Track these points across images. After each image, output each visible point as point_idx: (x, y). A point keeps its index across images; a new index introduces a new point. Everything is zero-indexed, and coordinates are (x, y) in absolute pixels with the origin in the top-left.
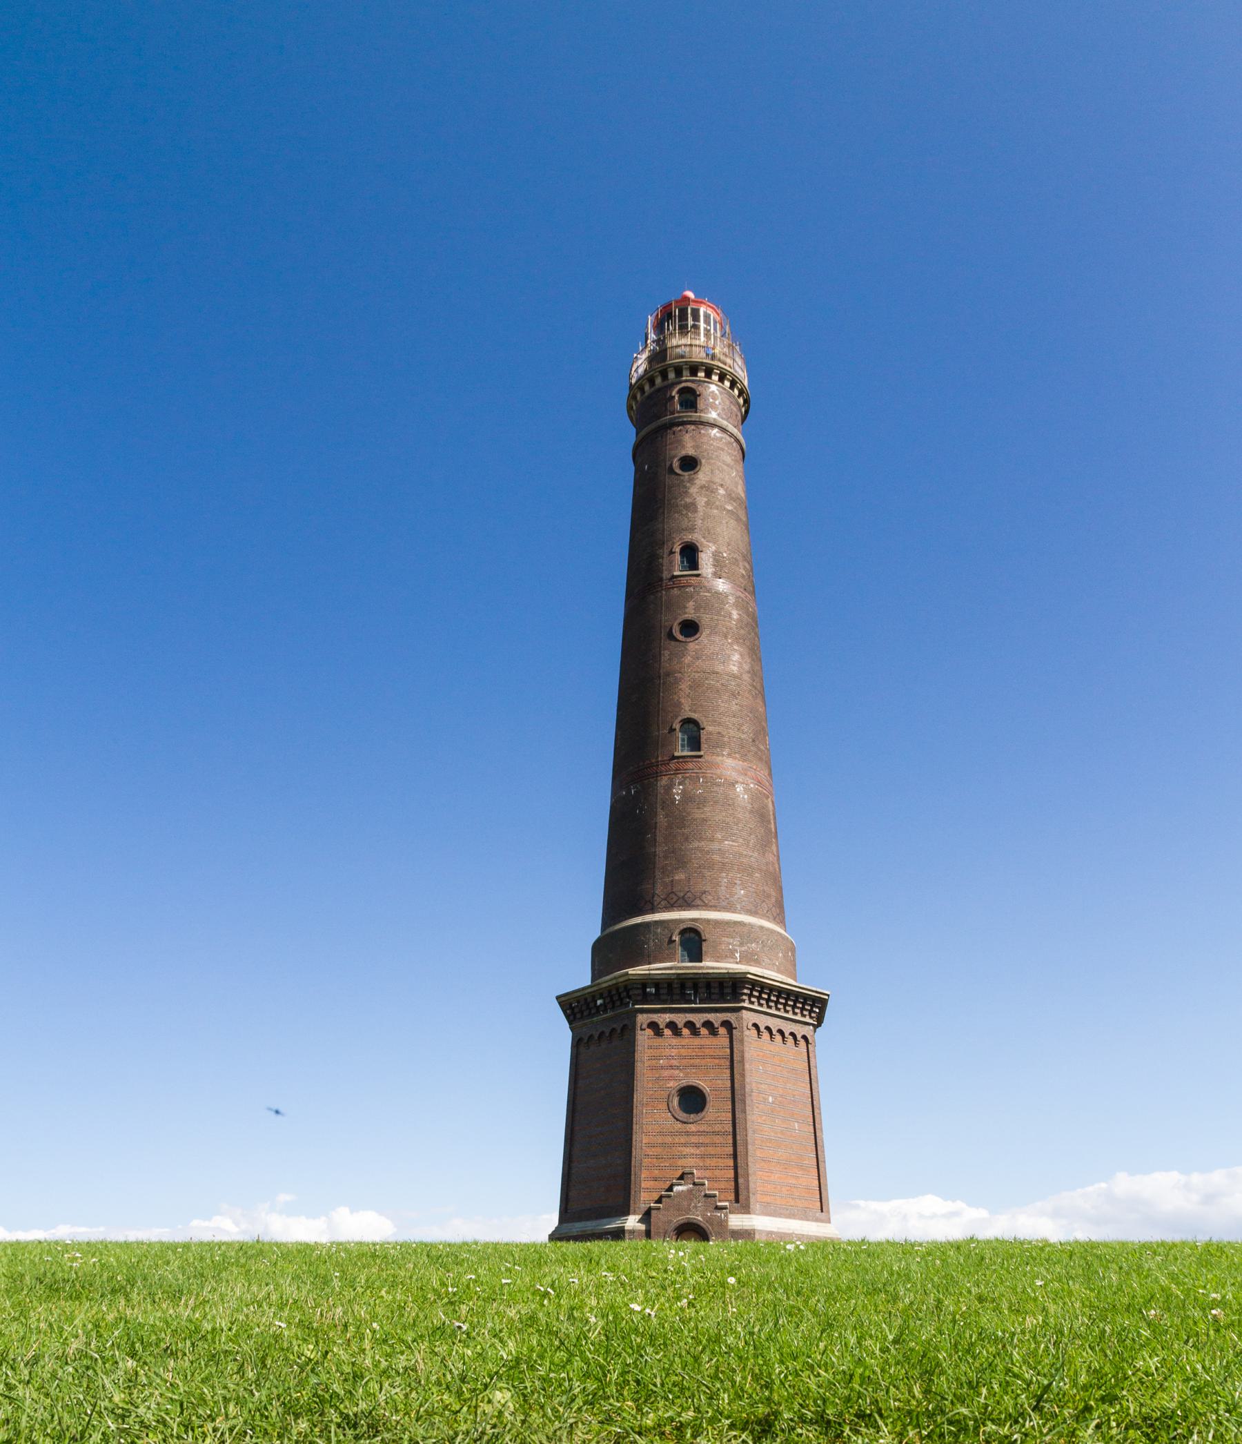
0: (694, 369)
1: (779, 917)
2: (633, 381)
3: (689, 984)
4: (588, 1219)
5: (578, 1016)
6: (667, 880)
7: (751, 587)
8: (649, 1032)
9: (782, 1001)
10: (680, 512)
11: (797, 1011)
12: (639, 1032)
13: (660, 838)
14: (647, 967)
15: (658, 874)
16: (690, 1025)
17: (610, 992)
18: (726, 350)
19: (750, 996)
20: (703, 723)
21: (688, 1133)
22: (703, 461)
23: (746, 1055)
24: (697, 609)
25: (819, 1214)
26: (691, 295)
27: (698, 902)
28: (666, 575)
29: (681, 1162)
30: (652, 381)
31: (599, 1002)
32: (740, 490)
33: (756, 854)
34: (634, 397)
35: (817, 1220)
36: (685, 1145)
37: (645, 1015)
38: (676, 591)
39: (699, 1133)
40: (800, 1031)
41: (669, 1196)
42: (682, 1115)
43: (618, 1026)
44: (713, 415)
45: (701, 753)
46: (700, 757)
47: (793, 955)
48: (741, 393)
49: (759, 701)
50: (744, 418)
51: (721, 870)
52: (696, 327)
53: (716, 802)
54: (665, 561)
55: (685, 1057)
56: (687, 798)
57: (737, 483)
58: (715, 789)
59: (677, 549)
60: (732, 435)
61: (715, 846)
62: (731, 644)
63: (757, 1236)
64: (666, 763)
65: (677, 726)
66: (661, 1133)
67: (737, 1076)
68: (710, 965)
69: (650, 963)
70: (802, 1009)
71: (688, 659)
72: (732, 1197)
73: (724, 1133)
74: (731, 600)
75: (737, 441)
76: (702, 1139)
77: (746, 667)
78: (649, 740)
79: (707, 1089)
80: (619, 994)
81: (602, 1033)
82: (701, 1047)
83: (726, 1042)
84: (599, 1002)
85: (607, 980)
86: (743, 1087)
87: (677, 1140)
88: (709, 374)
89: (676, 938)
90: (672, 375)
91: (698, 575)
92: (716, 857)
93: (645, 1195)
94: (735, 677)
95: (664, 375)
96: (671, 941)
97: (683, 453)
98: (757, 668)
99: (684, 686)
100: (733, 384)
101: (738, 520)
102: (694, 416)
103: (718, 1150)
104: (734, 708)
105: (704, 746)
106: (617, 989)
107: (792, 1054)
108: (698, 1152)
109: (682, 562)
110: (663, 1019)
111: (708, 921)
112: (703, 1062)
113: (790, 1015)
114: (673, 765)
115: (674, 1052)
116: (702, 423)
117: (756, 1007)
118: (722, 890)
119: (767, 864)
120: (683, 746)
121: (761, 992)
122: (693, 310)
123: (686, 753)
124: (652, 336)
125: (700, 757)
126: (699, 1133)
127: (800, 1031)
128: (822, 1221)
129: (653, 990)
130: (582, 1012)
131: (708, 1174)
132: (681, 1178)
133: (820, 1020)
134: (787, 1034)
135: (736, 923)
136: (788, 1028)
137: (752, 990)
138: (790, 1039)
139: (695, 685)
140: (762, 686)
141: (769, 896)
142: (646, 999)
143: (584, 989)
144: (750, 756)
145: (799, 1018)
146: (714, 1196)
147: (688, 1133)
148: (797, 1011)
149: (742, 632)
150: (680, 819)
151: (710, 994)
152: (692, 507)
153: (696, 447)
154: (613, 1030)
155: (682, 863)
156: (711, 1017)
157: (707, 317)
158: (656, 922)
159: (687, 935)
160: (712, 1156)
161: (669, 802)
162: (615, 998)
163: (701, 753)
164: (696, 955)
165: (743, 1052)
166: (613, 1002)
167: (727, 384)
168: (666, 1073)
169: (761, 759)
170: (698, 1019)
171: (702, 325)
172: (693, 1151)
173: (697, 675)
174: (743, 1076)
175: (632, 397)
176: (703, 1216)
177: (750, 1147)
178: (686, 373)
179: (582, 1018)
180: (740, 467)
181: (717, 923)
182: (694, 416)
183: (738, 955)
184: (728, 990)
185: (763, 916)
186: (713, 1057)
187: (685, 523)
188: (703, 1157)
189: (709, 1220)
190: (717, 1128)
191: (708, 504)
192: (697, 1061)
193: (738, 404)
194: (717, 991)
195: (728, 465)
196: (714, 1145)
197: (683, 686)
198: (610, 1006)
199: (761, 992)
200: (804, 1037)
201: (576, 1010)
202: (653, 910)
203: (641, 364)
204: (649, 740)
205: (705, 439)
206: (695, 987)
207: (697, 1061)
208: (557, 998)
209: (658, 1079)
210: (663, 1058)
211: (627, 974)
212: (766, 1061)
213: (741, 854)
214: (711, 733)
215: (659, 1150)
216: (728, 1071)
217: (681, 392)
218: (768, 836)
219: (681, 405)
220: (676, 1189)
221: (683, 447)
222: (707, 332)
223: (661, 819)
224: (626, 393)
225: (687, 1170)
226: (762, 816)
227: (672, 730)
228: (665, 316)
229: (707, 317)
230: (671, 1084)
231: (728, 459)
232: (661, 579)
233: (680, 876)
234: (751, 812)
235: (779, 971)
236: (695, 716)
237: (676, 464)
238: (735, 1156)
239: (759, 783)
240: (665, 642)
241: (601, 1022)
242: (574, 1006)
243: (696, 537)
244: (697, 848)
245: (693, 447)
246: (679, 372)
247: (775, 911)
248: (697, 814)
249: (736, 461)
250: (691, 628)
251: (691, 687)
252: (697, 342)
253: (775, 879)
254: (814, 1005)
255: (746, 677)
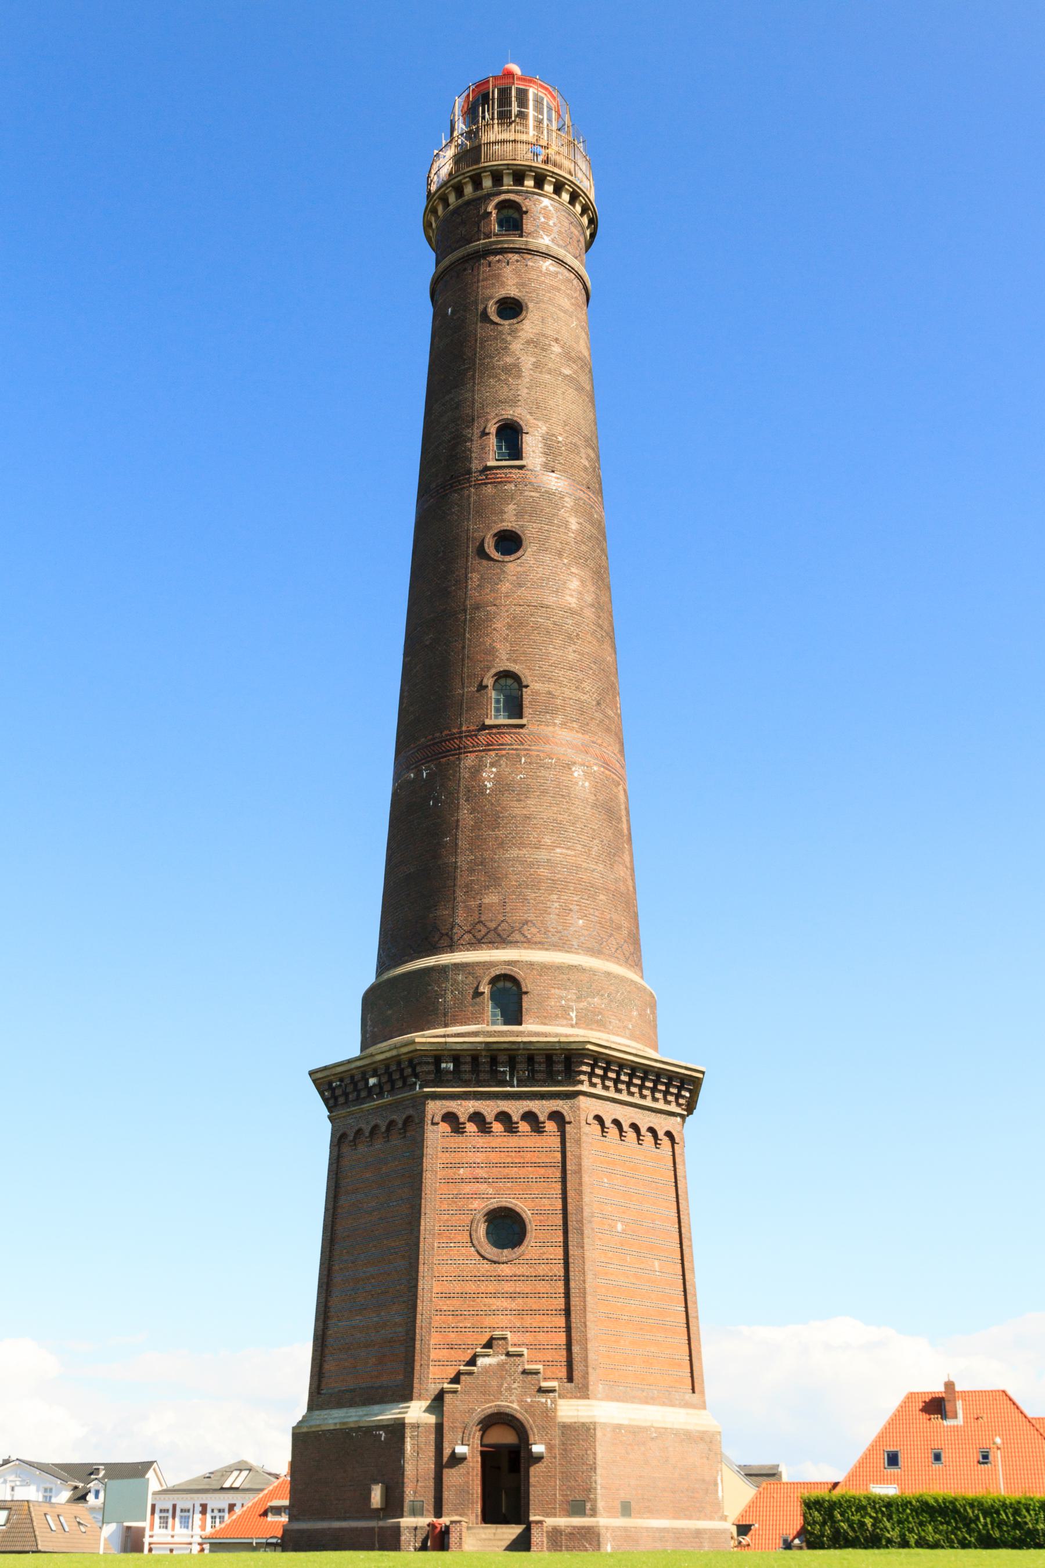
0: (519, 177)
1: (634, 958)
2: (433, 188)
3: (503, 1058)
4: (352, 1404)
5: (341, 1100)
6: (473, 904)
7: (595, 485)
8: (444, 1127)
9: (637, 1081)
10: (496, 376)
11: (658, 1095)
12: (429, 1128)
13: (463, 844)
14: (441, 1031)
15: (460, 894)
16: (504, 1117)
17: (387, 1067)
18: (564, 150)
19: (592, 1074)
20: (527, 677)
21: (499, 1278)
22: (531, 305)
23: (586, 1163)
24: (519, 515)
25: (689, 1396)
26: (516, 69)
27: (517, 936)
28: (476, 465)
29: (488, 1321)
30: (459, 190)
31: (372, 1081)
32: (583, 348)
33: (600, 867)
34: (434, 211)
35: (687, 1405)
36: (495, 1295)
37: (438, 1103)
38: (489, 490)
39: (515, 1278)
40: (662, 1124)
41: (471, 1373)
42: (490, 1251)
43: (399, 1118)
44: (544, 241)
45: (523, 721)
46: (522, 726)
47: (653, 1013)
48: (585, 210)
49: (607, 646)
50: (589, 245)
51: (551, 890)
52: (522, 116)
53: (544, 792)
54: (475, 446)
55: (496, 1165)
56: (503, 785)
57: (578, 337)
58: (543, 773)
59: (492, 429)
60: (571, 269)
61: (543, 855)
62: (568, 566)
63: (599, 1434)
64: (472, 735)
65: (489, 681)
66: (460, 1278)
67: (571, 1193)
68: (535, 1030)
69: (446, 1026)
70: (666, 1093)
71: (505, 587)
72: (563, 1373)
73: (552, 1278)
74: (569, 502)
75: (580, 277)
76: (520, 1287)
77: (589, 598)
78: (448, 701)
79: (527, 1214)
80: (402, 1071)
81: (376, 1127)
82: (520, 1150)
83: (556, 1142)
84: (372, 1081)
85: (385, 1049)
86: (580, 1210)
87: (483, 1288)
88: (540, 182)
89: (485, 988)
90: (487, 183)
91: (521, 467)
92: (544, 872)
93: (434, 1371)
94: (573, 612)
95: (477, 183)
96: (477, 994)
97: (502, 293)
98: (604, 599)
99: (500, 624)
100: (574, 197)
101: (580, 389)
102: (518, 242)
103: (544, 1304)
104: (572, 656)
105: (527, 711)
106: (399, 1063)
107: (652, 1158)
108: (514, 1306)
109: (500, 448)
110: (464, 1108)
111: (531, 965)
112: (522, 1172)
113: (648, 1102)
114: (483, 737)
115: (480, 1157)
116: (530, 252)
117: (599, 1091)
118: (552, 920)
119: (616, 880)
120: (497, 710)
121: (606, 1070)
122: (518, 89)
123: (502, 721)
124: (461, 126)
125: (522, 726)
126: (515, 1278)
127: (662, 1124)
128: (694, 1407)
129: (451, 1066)
130: (346, 1095)
131: (528, 1338)
132: (489, 1345)
133: (690, 1108)
134: (643, 1131)
135: (572, 968)
136: (645, 1121)
137: (593, 1066)
138: (648, 1138)
139: (517, 624)
140: (611, 624)
141: (619, 928)
142: (439, 1078)
143: (349, 1061)
144: (593, 726)
145: (661, 1105)
146: (537, 1373)
147: (499, 1278)
148: (658, 1095)
149: (584, 548)
150: (492, 818)
151: (533, 1071)
152: (514, 370)
153: (522, 285)
154: (392, 1123)
155: (495, 880)
156: (534, 1106)
157: (538, 102)
158: (456, 966)
159: (500, 985)
160: (533, 1312)
161: (475, 793)
162: (396, 1076)
163: (523, 721)
164: (513, 1015)
165: (580, 1157)
166: (392, 1082)
167: (566, 197)
168: (467, 1188)
169: (608, 730)
170: (516, 1109)
171: (531, 112)
172: (506, 1303)
173: (518, 609)
174: (580, 1193)
175: (430, 210)
176: (520, 1402)
177: (589, 1298)
178: (508, 181)
179: (346, 1102)
180: (582, 314)
181: (545, 968)
182: (518, 242)
183: (573, 1015)
184: (560, 1067)
185: (611, 957)
186: (537, 1165)
187: (504, 393)
188: (520, 1313)
189: (529, 1408)
190: (542, 1270)
191: (537, 366)
192: (513, 1172)
193: (581, 225)
194: (543, 1067)
195: (565, 312)
196: (537, 1295)
197: (498, 625)
198: (387, 1087)
199: (606, 1070)
200: (669, 1134)
201: (338, 1092)
202: (451, 948)
203: (444, 166)
204: (448, 701)
205: (533, 275)
206: (512, 1062)
207: (513, 1172)
208: (311, 1073)
209: (456, 1196)
210: (463, 1166)
211: (414, 1042)
212: (611, 1170)
213: (578, 867)
214: (537, 693)
215: (455, 1304)
216: (559, 1186)
217: (502, 206)
218: (619, 841)
219: (500, 225)
220: (480, 1361)
221: (503, 285)
222: (539, 122)
223: (465, 815)
224: (421, 204)
225: (497, 1333)
226: (610, 812)
227: (482, 687)
228: (479, 101)
229: (538, 102)
230: (476, 1204)
231: (566, 303)
232: (469, 472)
233: (491, 899)
234: (595, 806)
235: (632, 1037)
236: (515, 668)
237: (492, 310)
238: (568, 1312)
239: (606, 765)
240: (474, 561)
241: (375, 1111)
242: (336, 1087)
243: (519, 413)
244: (517, 859)
245: (517, 285)
246: (497, 178)
247: (628, 948)
248: (517, 809)
249: (577, 305)
250: (510, 542)
251: (509, 626)
252: (524, 137)
253: (628, 903)
254: (682, 1087)
255: (589, 613)
